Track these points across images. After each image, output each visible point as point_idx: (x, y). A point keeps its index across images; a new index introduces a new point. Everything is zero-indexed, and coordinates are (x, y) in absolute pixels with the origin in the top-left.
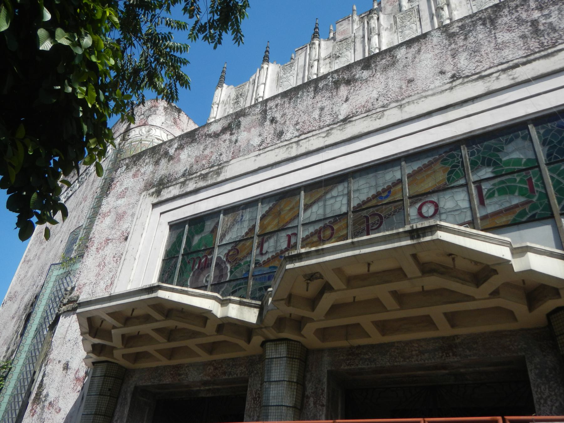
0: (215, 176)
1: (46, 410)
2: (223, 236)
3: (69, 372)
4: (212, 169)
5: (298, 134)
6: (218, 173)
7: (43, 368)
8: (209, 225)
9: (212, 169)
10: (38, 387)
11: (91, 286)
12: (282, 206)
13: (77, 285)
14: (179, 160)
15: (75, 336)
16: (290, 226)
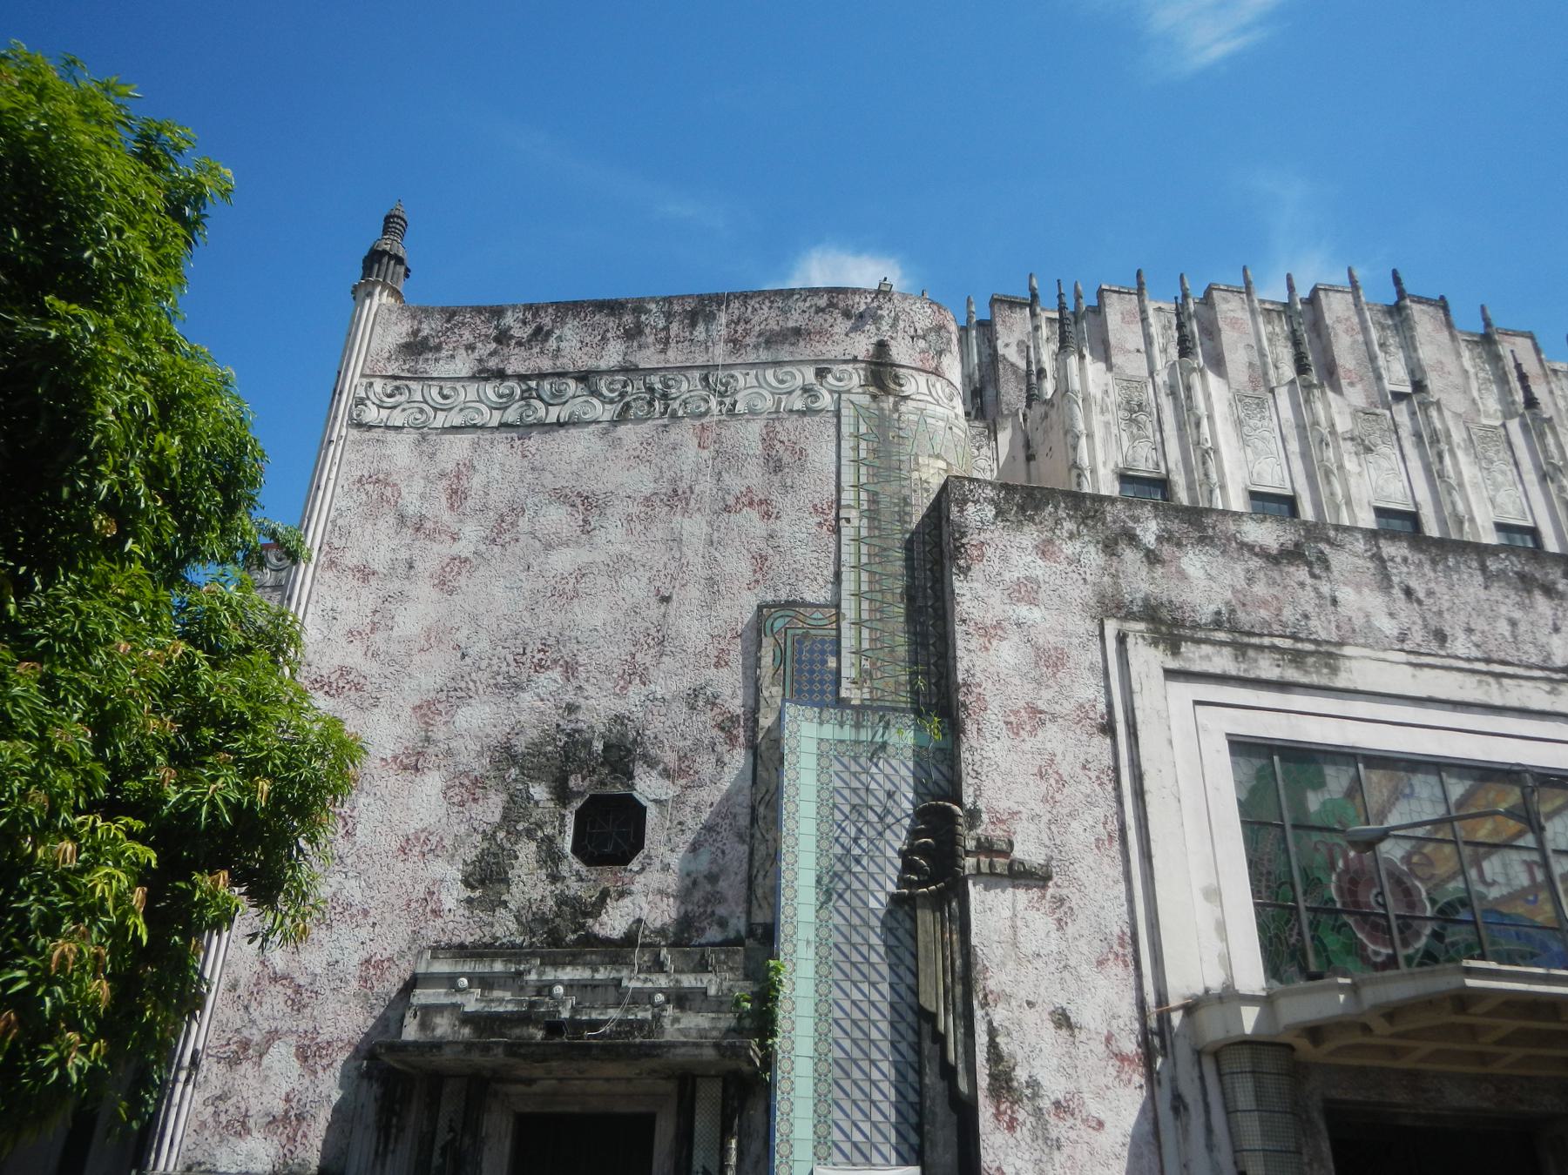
0: (1325, 671)
1: (1052, 1120)
3: (1082, 1036)
4: (1299, 646)
5: (1479, 655)
6: (1334, 671)
8: (1337, 780)
9: (1299, 646)
10: (988, 1060)
11: (1043, 826)
12: (1492, 795)
13: (981, 805)
14: (1183, 575)
15: (1055, 949)
16: (1521, 842)
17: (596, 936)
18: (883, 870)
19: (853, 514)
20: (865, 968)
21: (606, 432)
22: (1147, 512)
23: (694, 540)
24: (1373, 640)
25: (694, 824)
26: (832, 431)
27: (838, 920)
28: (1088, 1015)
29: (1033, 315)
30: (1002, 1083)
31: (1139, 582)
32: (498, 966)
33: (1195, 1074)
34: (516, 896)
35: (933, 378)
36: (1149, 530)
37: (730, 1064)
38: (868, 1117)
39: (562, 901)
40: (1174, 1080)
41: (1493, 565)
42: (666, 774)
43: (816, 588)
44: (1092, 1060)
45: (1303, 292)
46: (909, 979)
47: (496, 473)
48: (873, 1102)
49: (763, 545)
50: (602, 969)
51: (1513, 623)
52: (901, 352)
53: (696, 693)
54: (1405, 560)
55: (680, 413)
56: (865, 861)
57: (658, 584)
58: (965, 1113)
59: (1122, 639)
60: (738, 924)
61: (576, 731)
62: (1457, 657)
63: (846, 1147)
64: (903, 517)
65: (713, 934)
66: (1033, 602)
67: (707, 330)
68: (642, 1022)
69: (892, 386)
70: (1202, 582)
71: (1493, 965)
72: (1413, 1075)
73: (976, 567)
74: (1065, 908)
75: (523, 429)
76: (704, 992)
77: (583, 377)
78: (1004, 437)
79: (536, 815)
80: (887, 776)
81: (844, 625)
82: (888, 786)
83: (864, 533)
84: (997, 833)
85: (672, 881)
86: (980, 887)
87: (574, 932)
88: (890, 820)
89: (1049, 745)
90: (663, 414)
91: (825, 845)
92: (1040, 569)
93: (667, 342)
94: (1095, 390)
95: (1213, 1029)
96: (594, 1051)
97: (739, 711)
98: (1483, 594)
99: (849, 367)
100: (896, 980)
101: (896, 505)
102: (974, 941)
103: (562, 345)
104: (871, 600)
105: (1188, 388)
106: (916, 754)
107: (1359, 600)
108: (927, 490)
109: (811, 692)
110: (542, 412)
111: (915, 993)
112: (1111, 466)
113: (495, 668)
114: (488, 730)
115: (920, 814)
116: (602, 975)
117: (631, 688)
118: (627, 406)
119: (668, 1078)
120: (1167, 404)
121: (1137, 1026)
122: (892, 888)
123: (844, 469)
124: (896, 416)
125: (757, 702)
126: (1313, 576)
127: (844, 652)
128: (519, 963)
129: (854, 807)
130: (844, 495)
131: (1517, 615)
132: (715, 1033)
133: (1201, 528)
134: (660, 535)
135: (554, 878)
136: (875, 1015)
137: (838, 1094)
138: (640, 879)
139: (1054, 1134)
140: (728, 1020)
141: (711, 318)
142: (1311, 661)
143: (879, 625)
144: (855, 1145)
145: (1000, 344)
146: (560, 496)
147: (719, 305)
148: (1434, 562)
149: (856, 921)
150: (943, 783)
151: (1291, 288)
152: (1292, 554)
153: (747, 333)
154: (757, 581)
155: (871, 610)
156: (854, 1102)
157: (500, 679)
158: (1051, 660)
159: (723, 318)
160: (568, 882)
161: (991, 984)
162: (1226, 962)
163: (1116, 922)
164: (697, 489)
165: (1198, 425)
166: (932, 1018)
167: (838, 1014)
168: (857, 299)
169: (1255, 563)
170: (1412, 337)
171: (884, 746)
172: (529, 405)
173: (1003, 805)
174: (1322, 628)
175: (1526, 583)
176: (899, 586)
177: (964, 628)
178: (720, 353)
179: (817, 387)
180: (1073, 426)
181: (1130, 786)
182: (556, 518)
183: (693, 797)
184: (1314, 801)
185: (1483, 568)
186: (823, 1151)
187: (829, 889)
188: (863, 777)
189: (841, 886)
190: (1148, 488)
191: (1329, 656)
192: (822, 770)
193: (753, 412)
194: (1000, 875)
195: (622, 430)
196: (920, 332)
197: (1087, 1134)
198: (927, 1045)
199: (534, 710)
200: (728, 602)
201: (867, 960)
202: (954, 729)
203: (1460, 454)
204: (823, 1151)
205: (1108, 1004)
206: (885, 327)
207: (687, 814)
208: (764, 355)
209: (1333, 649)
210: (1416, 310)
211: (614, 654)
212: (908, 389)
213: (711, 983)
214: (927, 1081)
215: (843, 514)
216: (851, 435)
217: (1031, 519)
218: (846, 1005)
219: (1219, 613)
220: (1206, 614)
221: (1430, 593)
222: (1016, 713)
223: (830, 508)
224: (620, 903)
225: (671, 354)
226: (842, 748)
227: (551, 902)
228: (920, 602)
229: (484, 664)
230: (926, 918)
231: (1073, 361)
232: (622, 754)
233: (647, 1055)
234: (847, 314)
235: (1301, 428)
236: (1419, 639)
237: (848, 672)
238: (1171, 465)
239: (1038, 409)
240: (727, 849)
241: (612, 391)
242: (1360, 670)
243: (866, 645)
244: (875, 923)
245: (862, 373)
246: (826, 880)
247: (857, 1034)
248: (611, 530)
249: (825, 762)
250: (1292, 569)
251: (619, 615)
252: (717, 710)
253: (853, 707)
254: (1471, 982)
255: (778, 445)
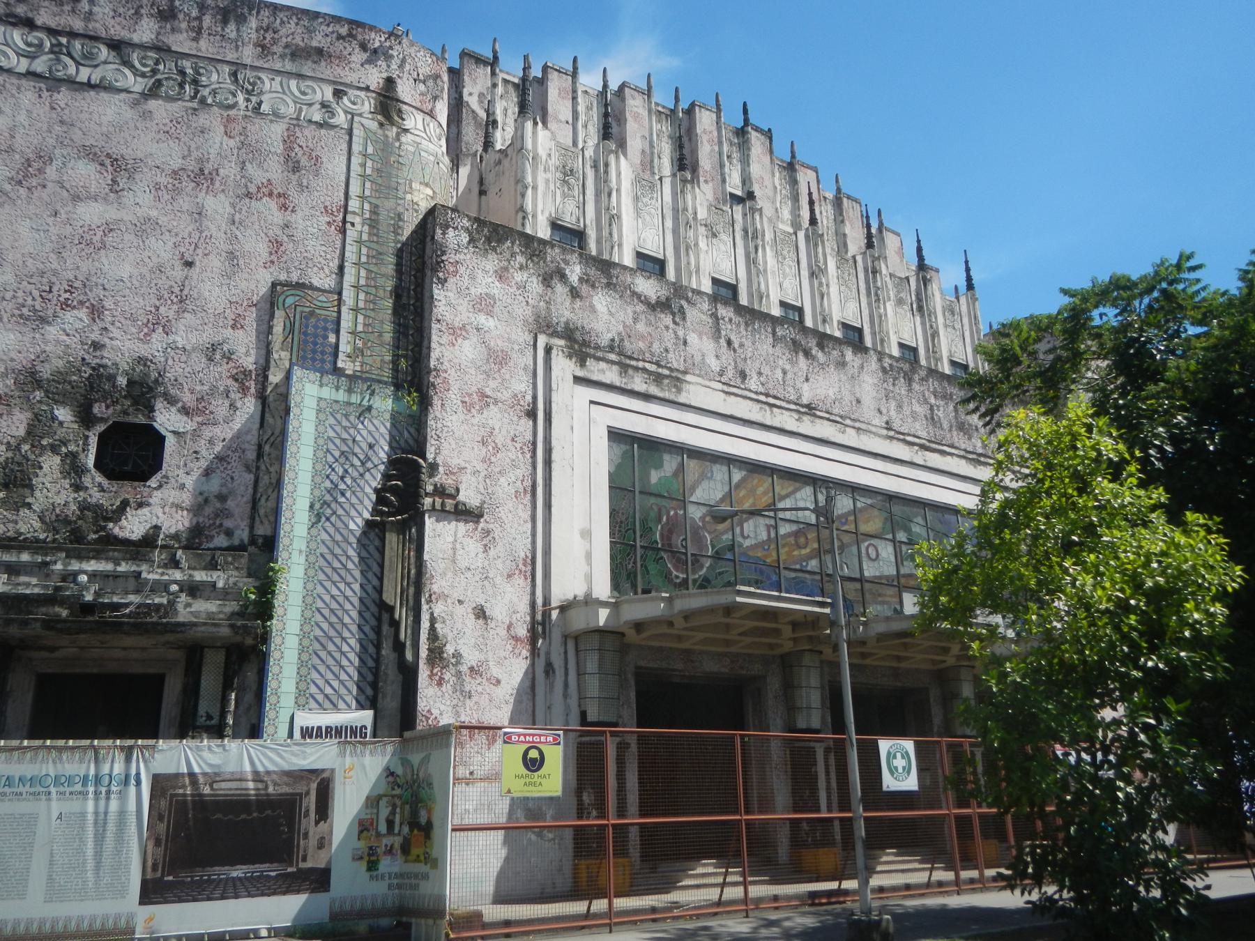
1: (468, 679)
2: (693, 489)
3: (492, 625)
4: (660, 370)
6: (679, 390)
7: (425, 607)
8: (670, 463)
9: (660, 370)
12: (756, 481)
13: (439, 460)
14: (593, 309)
15: (480, 565)
17: (116, 537)
18: (362, 502)
19: (357, 220)
20: (343, 572)
21: (136, 103)
22: (574, 258)
23: (218, 217)
24: (705, 374)
25: (207, 455)
26: (344, 147)
27: (325, 536)
28: (498, 611)
29: (493, 74)
30: (436, 655)
31: (564, 310)
32: (25, 557)
33: (562, 651)
34: (39, 500)
35: (428, 118)
36: (575, 272)
37: (238, 639)
38: (337, 677)
39: (84, 507)
40: (548, 654)
41: (780, 332)
42: (185, 411)
43: (322, 275)
44: (498, 640)
45: (684, 105)
46: (376, 582)
47: (22, 118)
48: (342, 667)
49: (279, 232)
50: (123, 564)
51: (784, 372)
52: (405, 90)
53: (214, 347)
54: (731, 320)
55: (210, 101)
56: (348, 494)
57: (183, 250)
58: (409, 676)
59: (548, 350)
60: (243, 534)
61: (100, 366)
62: (750, 391)
63: (320, 697)
64: (396, 230)
65: (221, 541)
66: (490, 314)
67: (238, 30)
68: (158, 607)
69: (396, 118)
70: (605, 315)
71: (752, 589)
72: (687, 652)
73: (451, 280)
74: (490, 538)
75: (53, 82)
76: (214, 585)
77: (116, 46)
78: (464, 171)
79: (61, 433)
80: (369, 432)
81: (344, 309)
82: (370, 440)
83: (365, 237)
84: (449, 482)
85: (186, 498)
86: (433, 519)
87: (95, 533)
88: (369, 465)
89: (490, 422)
90: (193, 98)
91: (318, 480)
92: (497, 289)
93: (199, 31)
94: (542, 152)
95: (578, 622)
96: (125, 628)
97: (252, 367)
98: (771, 350)
99: (362, 94)
100: (365, 582)
101: (392, 218)
102: (426, 557)
103: (96, 9)
104: (367, 293)
105: (607, 165)
106: (393, 417)
107: (701, 345)
108: (417, 211)
109: (314, 360)
110: (72, 70)
111: (380, 591)
112: (547, 214)
113: (20, 300)
114: (13, 355)
115: (392, 463)
116: (123, 568)
117: (154, 335)
118: (159, 83)
119: (179, 648)
120: (590, 174)
121: (528, 618)
122: (367, 515)
123: (352, 181)
124: (397, 144)
125: (267, 361)
126: (675, 323)
127: (343, 332)
128: (46, 555)
129: (343, 453)
130: (351, 203)
131: (788, 367)
132: (221, 616)
133: (609, 276)
134: (186, 207)
135: (77, 487)
136: (348, 606)
137: (316, 661)
138: (158, 494)
139: (467, 689)
140: (232, 606)
141: (241, 20)
142: (665, 381)
143: (372, 314)
144: (326, 696)
145: (465, 92)
146: (90, 153)
147: (250, 9)
148: (747, 324)
149: (338, 538)
150: (411, 442)
151: (677, 99)
152: (663, 306)
153: (274, 42)
154: (272, 262)
155: (366, 301)
156: (328, 667)
157: (25, 311)
158: (497, 359)
159: (253, 23)
160: (91, 492)
161: (435, 588)
162: (589, 578)
163: (523, 549)
164: (221, 171)
165: (610, 195)
166: (391, 609)
167: (320, 604)
168: (373, 35)
169: (640, 308)
170: (748, 155)
171: (369, 409)
172: (58, 60)
173: (455, 462)
174: (675, 361)
175: (796, 346)
176: (389, 285)
177: (438, 326)
178: (248, 54)
179: (334, 105)
180: (524, 177)
181: (542, 455)
182: (84, 173)
183: (207, 432)
184: (654, 476)
185: (774, 333)
186: (302, 700)
187: (319, 514)
188: (352, 431)
189: (329, 511)
190: (571, 236)
191: (677, 380)
192: (320, 422)
193: (276, 115)
194: (449, 512)
195: (153, 104)
196: (421, 77)
197: (489, 688)
198: (386, 628)
199: (62, 340)
200: (246, 276)
201: (345, 567)
202: (425, 403)
203: (768, 249)
204: (302, 700)
205: (510, 605)
206: (394, 66)
207: (202, 445)
208: (289, 66)
209: (680, 376)
210: (754, 136)
211: (140, 304)
212: (408, 124)
213: (219, 579)
214: (383, 652)
215: (349, 218)
216: (360, 153)
217: (494, 249)
218: (327, 598)
219: (613, 340)
220: (604, 341)
221: (742, 345)
222: (470, 395)
223: (338, 211)
224: (139, 512)
225: (203, 44)
226: (336, 407)
227: (74, 507)
228: (404, 300)
229: (8, 295)
230: (392, 539)
231: (529, 125)
232: (144, 389)
233: (172, 632)
234: (364, 47)
235: (675, 210)
236: (730, 376)
237: (344, 347)
238: (588, 222)
239: (491, 157)
240: (236, 475)
241: (144, 65)
242: (696, 392)
243: (360, 328)
244: (353, 540)
245: (372, 101)
246: (317, 506)
247: (334, 619)
248: (139, 193)
249: (322, 416)
250: (663, 316)
251: (145, 271)
252: (231, 364)
253: (347, 376)
254: (739, 599)
255: (297, 149)
